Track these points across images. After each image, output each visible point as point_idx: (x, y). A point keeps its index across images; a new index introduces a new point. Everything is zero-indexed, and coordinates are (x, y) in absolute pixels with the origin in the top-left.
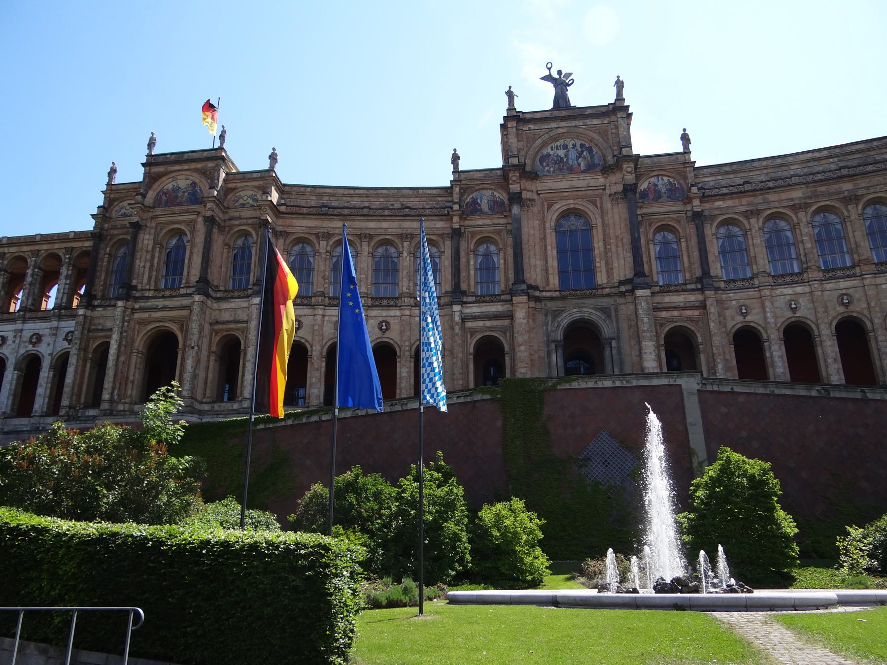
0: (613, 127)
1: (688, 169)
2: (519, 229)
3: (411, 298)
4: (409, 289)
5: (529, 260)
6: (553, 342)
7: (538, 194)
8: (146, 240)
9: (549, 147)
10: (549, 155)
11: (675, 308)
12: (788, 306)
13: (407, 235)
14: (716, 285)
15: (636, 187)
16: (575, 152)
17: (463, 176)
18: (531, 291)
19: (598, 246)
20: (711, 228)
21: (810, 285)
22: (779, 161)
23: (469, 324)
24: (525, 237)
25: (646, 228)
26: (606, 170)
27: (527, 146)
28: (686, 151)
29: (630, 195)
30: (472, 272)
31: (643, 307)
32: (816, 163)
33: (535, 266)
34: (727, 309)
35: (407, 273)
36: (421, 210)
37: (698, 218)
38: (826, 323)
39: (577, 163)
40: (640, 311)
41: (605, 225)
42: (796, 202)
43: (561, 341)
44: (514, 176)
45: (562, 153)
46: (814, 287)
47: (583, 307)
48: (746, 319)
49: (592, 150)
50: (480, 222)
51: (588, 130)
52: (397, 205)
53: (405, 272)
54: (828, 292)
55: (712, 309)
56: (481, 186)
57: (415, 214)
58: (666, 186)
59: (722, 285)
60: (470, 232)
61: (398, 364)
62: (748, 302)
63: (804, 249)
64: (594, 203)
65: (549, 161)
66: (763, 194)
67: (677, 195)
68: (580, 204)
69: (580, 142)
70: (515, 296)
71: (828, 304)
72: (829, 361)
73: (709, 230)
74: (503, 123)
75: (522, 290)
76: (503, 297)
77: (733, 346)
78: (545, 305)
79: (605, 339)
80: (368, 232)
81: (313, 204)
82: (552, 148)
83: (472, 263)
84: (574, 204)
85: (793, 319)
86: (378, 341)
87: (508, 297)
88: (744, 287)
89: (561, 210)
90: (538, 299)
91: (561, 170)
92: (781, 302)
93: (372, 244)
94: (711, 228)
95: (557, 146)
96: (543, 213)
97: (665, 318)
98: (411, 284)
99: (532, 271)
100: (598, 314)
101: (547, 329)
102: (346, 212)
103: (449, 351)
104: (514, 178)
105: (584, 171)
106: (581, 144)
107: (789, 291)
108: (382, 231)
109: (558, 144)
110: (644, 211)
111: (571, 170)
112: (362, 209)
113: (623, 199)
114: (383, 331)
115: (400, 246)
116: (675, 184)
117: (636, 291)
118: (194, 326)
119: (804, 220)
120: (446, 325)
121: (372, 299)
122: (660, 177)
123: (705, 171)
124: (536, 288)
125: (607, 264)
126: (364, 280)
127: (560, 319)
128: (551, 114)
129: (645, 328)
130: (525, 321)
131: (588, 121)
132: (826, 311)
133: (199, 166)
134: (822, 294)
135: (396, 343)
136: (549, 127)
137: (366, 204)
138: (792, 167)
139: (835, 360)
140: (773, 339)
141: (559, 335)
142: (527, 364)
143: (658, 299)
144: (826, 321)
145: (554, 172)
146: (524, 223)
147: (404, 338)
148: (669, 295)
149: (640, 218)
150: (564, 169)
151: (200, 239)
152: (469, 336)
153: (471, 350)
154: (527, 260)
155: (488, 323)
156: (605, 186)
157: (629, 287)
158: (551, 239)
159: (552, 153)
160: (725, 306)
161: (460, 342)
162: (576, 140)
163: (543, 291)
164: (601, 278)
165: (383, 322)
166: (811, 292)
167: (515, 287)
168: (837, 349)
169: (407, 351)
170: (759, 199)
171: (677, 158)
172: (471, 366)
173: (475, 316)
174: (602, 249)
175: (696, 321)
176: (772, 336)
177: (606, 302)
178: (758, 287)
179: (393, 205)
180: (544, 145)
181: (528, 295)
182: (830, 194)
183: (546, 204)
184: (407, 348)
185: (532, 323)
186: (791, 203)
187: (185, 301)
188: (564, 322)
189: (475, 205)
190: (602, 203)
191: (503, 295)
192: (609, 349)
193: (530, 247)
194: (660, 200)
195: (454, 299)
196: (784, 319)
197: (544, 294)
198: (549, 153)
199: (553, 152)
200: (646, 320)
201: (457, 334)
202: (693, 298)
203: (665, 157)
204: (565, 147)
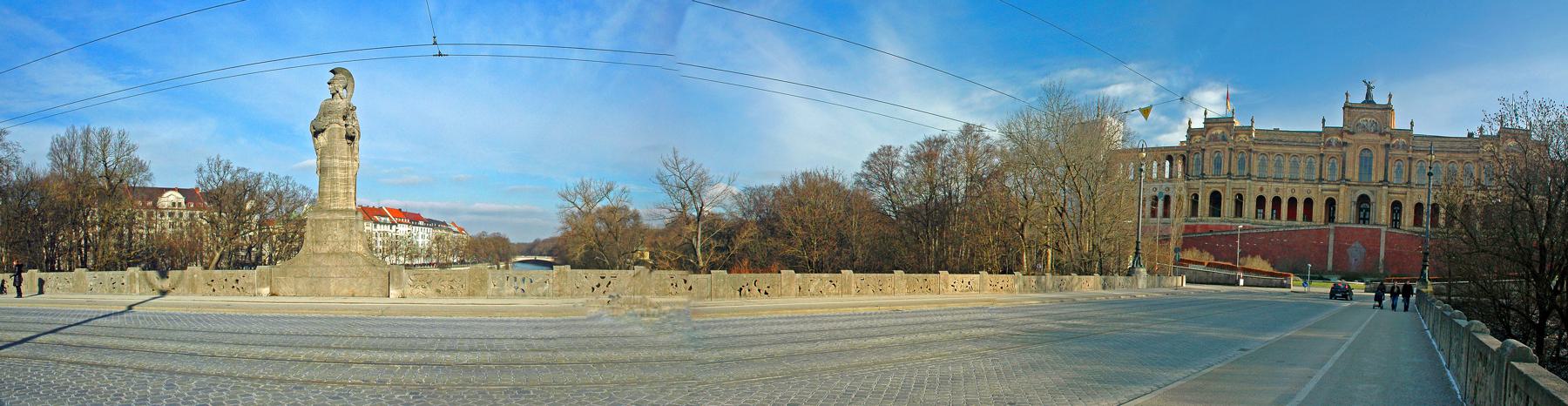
8: (1207, 155)
19: (1374, 165)
23: (1324, 192)
24: (1347, 160)
26: (1382, 134)
31: (1385, 193)
37: (1410, 159)
41: (1377, 157)
44: (1345, 134)
45: (1365, 123)
52: (1300, 140)
55: (1408, 195)
57: (1303, 144)
73: (1414, 164)
81: (1267, 138)
90: (1349, 185)
111: (1368, 131)
118: (1228, 191)
133: (1225, 124)
137: (1287, 139)
141: (1356, 200)
143: (1391, 189)
146: (1347, 154)
151: (1227, 156)
155: (1331, 192)
158: (1357, 160)
164: (1373, 179)
172: (1324, 208)
175: (1402, 199)
177: (1373, 188)
180: (1359, 119)
181: (1346, 184)
182: (1455, 157)
187: (1224, 180)
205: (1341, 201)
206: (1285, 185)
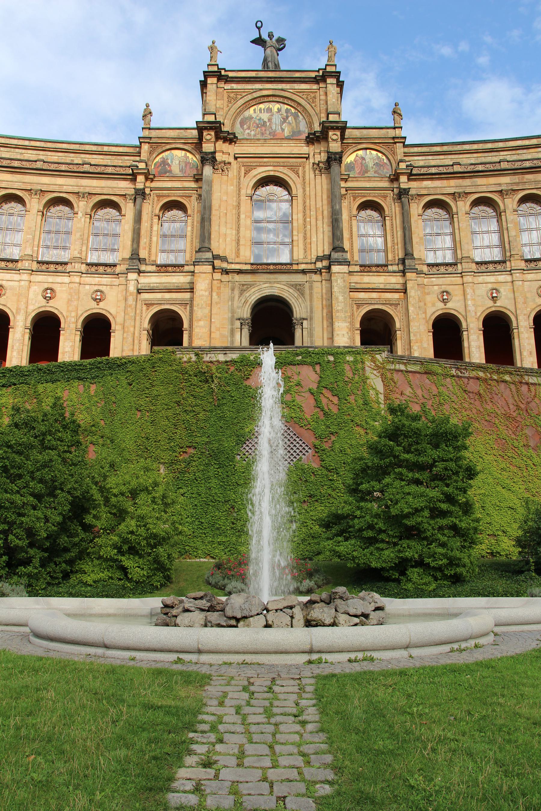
0: (322, 93)
1: (397, 144)
2: (209, 192)
3: (82, 263)
4: (81, 254)
5: (219, 229)
6: (239, 319)
7: (236, 158)
9: (252, 109)
10: (251, 118)
11: (373, 290)
12: (489, 295)
13: (84, 194)
14: (419, 267)
15: (341, 158)
16: (280, 116)
17: (154, 134)
18: (217, 263)
20: (418, 208)
21: (511, 274)
22: (489, 146)
24: (215, 203)
25: (350, 202)
27: (228, 106)
28: (397, 125)
29: (335, 166)
30: (154, 239)
32: (525, 151)
33: (226, 235)
34: (428, 294)
35: (81, 236)
36: (103, 168)
38: (525, 315)
39: (281, 128)
40: (335, 289)
42: (503, 188)
43: (247, 320)
45: (265, 116)
46: (516, 277)
47: (275, 282)
48: (447, 307)
49: (298, 116)
50: (169, 185)
51: (294, 94)
53: (78, 235)
54: (528, 283)
55: (411, 292)
56: (173, 146)
58: (374, 160)
59: (425, 269)
60: (156, 194)
61: (61, 338)
62: (448, 288)
63: (509, 237)
64: (297, 173)
65: (250, 123)
66: (470, 177)
67: (385, 170)
68: (281, 172)
69: (286, 106)
70: (197, 265)
71: (528, 295)
72: (525, 353)
73: (416, 208)
74: (203, 79)
75: (207, 259)
76: (186, 268)
77: (431, 334)
78: (233, 278)
79: (296, 319)
80: (39, 188)
82: (255, 110)
83: (155, 228)
84: (275, 171)
85: (493, 309)
86: (41, 310)
87: (191, 268)
88: (447, 272)
89: (259, 177)
90: (226, 272)
91: (263, 134)
92: (483, 290)
93: (44, 201)
94: (418, 208)
95: (260, 109)
96: (239, 179)
97: (363, 299)
98: (84, 248)
99: (221, 241)
100: (291, 291)
101: (232, 304)
102: (16, 164)
103: (121, 324)
104: (208, 137)
105: (288, 139)
106: (287, 109)
107: (491, 279)
108: (57, 188)
109: (262, 106)
110: (349, 184)
112: (36, 161)
113: (326, 169)
114: (48, 299)
115: (75, 205)
116: (383, 160)
117: (332, 266)
119: (510, 206)
120: (120, 295)
121: (39, 262)
122: (368, 151)
123: (416, 150)
124: (224, 259)
125: (305, 238)
126: (30, 242)
127: (248, 295)
128: (256, 74)
129: (339, 308)
130: (207, 293)
131: (296, 85)
132: (525, 303)
134: (523, 284)
135: (61, 313)
136: (254, 87)
138: (502, 153)
139: (531, 353)
140: (472, 329)
141: (246, 313)
142: (205, 341)
143: (356, 278)
144: (525, 312)
145: (255, 136)
146: (216, 187)
147: (70, 309)
148: (369, 275)
149: (343, 191)
150: (266, 133)
152: (145, 307)
153: (146, 324)
154: (217, 228)
155: (167, 296)
156: (309, 154)
157: (325, 263)
159: (254, 116)
160: (426, 291)
161: (133, 314)
162: (282, 105)
163: (232, 263)
165: (47, 289)
166: (512, 282)
167: (200, 255)
168: (533, 341)
169: (73, 323)
170: (467, 182)
171: (388, 132)
173: (153, 287)
174: (301, 221)
176: (471, 325)
177: (299, 278)
178: (461, 273)
179: (72, 160)
180: (247, 105)
183: (243, 168)
184: (73, 320)
185: (216, 297)
186: (499, 189)
188: (252, 298)
189: (164, 165)
190: (304, 172)
191: (188, 265)
192: (300, 331)
193: (222, 214)
194: (366, 175)
195: (130, 266)
196: (484, 308)
197: (233, 267)
198: (251, 116)
199: (256, 115)
200: (341, 298)
201: (130, 306)
202: (395, 280)
203: (375, 130)
204: (269, 110)
205: (199, 313)
206: (25, 277)
